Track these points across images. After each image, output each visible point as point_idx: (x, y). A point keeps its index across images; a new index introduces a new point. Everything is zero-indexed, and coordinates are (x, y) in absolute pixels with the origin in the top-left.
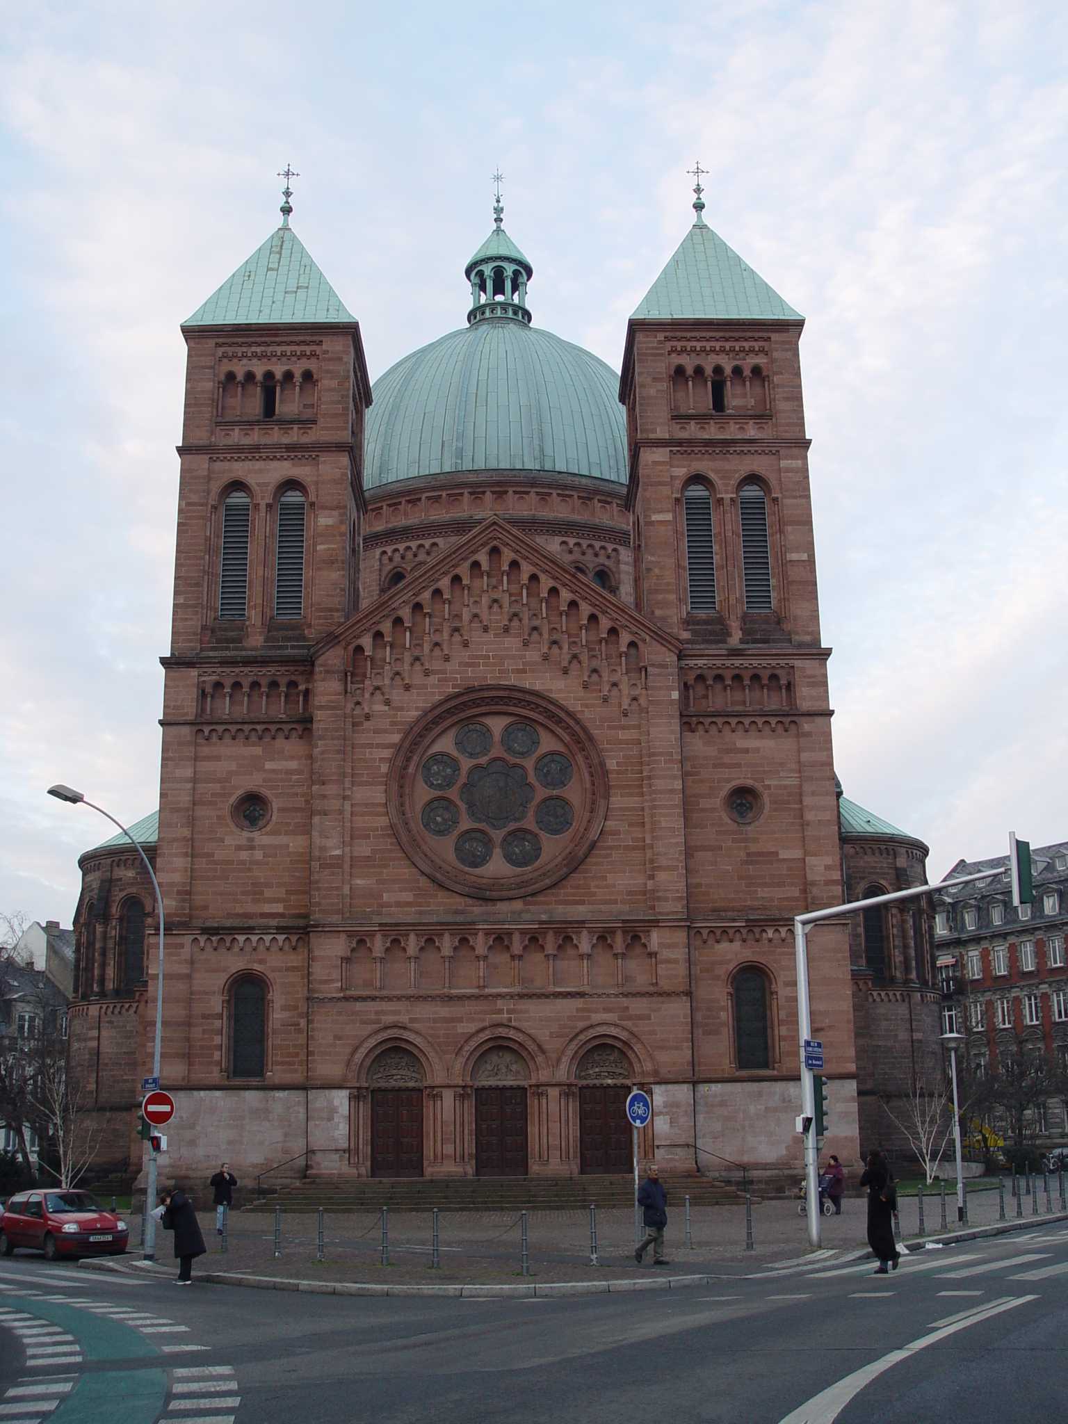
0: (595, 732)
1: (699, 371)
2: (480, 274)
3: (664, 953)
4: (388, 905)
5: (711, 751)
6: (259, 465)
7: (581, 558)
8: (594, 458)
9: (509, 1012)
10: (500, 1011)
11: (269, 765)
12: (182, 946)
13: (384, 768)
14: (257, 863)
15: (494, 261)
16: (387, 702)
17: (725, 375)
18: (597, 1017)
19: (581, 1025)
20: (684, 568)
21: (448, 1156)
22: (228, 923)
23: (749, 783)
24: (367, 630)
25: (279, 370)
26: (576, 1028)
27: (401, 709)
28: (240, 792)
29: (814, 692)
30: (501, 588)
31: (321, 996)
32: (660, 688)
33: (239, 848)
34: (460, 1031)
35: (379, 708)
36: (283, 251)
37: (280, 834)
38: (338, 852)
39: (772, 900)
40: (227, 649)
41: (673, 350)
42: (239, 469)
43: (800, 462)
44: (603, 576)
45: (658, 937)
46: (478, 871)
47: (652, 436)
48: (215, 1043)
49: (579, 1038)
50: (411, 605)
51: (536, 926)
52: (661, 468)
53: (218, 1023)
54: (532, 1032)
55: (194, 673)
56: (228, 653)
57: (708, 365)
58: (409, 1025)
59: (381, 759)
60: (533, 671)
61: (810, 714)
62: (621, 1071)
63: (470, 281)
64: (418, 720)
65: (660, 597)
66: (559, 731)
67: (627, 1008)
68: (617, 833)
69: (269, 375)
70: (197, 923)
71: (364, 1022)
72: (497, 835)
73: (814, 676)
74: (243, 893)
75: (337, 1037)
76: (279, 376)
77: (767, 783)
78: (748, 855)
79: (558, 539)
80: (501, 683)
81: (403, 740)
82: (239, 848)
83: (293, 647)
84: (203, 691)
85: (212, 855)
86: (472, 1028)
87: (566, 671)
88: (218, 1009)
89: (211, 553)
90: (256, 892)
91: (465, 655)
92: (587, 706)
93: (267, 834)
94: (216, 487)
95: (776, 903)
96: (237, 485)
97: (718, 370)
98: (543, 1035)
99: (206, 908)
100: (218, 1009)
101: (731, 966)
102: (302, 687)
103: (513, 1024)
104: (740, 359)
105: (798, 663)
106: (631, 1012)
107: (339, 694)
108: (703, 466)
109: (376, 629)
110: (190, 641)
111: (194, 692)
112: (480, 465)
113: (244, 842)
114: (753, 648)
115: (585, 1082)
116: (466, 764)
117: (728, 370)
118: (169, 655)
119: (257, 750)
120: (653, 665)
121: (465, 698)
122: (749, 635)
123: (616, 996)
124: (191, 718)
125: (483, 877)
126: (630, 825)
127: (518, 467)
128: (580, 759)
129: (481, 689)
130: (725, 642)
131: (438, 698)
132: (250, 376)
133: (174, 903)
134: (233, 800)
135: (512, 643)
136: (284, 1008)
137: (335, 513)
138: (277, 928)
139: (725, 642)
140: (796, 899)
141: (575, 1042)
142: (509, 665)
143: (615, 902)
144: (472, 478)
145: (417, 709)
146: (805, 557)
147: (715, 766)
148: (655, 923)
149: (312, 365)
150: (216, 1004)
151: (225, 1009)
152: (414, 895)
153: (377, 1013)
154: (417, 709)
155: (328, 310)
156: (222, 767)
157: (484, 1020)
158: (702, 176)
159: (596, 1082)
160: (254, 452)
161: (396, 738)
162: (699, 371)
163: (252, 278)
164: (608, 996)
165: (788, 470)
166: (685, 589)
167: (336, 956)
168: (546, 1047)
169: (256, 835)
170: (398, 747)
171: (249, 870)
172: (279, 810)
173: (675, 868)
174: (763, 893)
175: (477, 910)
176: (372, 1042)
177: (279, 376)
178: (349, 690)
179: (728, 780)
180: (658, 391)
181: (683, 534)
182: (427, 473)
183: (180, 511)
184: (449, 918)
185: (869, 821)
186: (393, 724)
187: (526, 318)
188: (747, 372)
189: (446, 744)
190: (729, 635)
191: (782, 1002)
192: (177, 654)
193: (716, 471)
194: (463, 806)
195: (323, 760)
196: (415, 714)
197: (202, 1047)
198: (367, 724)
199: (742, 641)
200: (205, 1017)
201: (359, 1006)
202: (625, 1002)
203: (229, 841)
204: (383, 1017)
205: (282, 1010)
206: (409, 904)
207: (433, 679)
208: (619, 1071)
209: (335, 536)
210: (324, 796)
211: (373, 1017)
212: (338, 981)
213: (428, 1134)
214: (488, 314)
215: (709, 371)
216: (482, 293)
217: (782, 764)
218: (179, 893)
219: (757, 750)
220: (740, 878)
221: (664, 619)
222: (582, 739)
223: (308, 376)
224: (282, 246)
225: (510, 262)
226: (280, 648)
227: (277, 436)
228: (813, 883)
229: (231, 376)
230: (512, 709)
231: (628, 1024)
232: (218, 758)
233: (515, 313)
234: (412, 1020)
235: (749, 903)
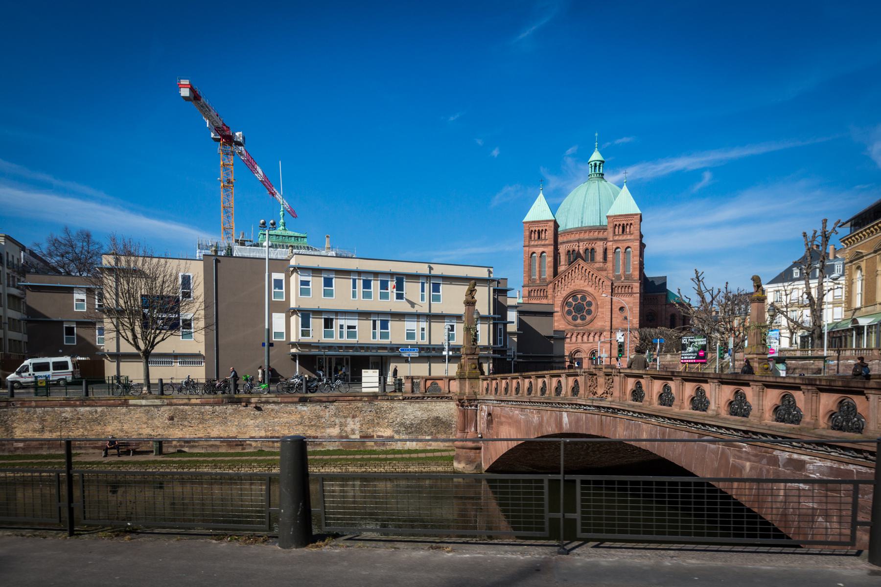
35: (559, 294)
42: (534, 249)
69: (539, 230)
72: (579, 316)
97: (623, 224)
98: (585, 349)
111: (527, 292)
112: (587, 225)
114: (625, 281)
116: (574, 303)
132: (535, 231)
135: (582, 282)
142: (581, 286)
144: (584, 228)
148: (605, 331)
149: (547, 228)
160: (537, 246)
161: (562, 299)
175: (575, 328)
189: (571, 300)
222: (595, 298)
223: (546, 230)
227: (540, 242)
229: (532, 231)
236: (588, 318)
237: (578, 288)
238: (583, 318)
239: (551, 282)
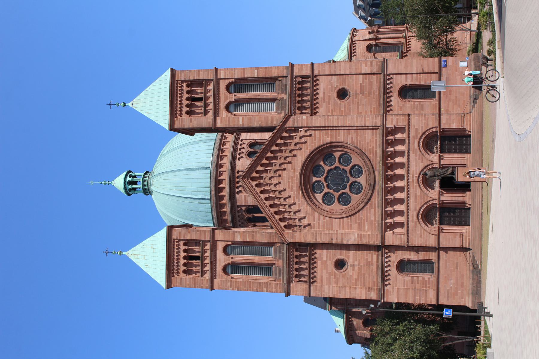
0: (316, 146)
1: (187, 106)
2: (130, 190)
3: (394, 123)
4: (375, 218)
5: (324, 105)
6: (218, 262)
7: (245, 154)
8: (206, 148)
9: (413, 176)
10: (413, 180)
11: (325, 259)
12: (387, 290)
13: (327, 219)
14: (359, 263)
15: (126, 185)
16: (304, 218)
17: (189, 97)
18: (416, 147)
19: (419, 152)
20: (259, 113)
21: (463, 199)
22: (380, 274)
23: (336, 92)
24: (279, 224)
25: (183, 254)
27: (306, 212)
28: (334, 269)
29: (304, 69)
30: (265, 177)
31: (406, 242)
32: (302, 123)
33: (353, 270)
34: (420, 194)
36: (137, 254)
37: (349, 255)
38: (356, 235)
39: (377, 85)
40: (283, 273)
41: (181, 114)
43: (222, 71)
44: (251, 145)
45: (389, 125)
46: (364, 187)
47: (211, 123)
48: (422, 279)
49: (423, 153)
50: (270, 208)
51: (384, 167)
52: (223, 121)
53: (415, 278)
54: (420, 170)
55: (291, 284)
56: (285, 273)
57: (185, 102)
58: (417, 211)
59: (324, 219)
60: (294, 167)
61: (313, 70)
62: (435, 139)
63: (132, 194)
64: (310, 206)
65: (269, 122)
66: (315, 158)
67: (413, 136)
68: (352, 138)
69: (185, 258)
70: (380, 284)
71: (416, 227)
73: (299, 69)
74: (369, 267)
75: (421, 236)
76: (185, 254)
77: (336, 86)
78: (361, 93)
79: (237, 161)
80: (298, 177)
81: (317, 212)
82: (353, 270)
83: (283, 250)
84: (298, 282)
85: (356, 279)
86: (418, 189)
87: (295, 156)
88: (410, 278)
89: (248, 278)
90: (370, 264)
91: (287, 189)
92: (307, 148)
93: (349, 259)
94: (225, 277)
95: (378, 84)
96: (225, 269)
97: (187, 99)
98: (422, 166)
99: (374, 282)
100: (410, 278)
101: (400, 100)
102: (298, 247)
103: (418, 175)
104: (184, 92)
105: (295, 74)
106: (415, 135)
107: (301, 234)
108: (222, 105)
109: (278, 220)
110: (280, 286)
111: (299, 284)
113: (352, 268)
115: (439, 152)
116: (326, 190)
117: (188, 96)
118: (285, 294)
119: (319, 263)
120: (294, 124)
121: (304, 190)
122: (284, 91)
123: (409, 140)
124: (307, 286)
125: (366, 185)
126: (349, 134)
127: (209, 175)
128: (325, 151)
129: (301, 184)
130: (286, 100)
131: (303, 199)
132: (185, 265)
133: (372, 293)
134: (336, 272)
136: (410, 255)
137: (236, 234)
138: (382, 256)
139: (286, 100)
140: (377, 78)
141: (424, 154)
142: (292, 174)
143: (376, 140)
144: (213, 193)
145: (306, 207)
146: (256, 71)
147: (329, 104)
148: (384, 125)
150: (408, 279)
151: (410, 275)
152: (372, 209)
153: (413, 222)
154: (306, 207)
155: (161, 237)
156: (325, 275)
157: (416, 186)
158: (112, 103)
159: (438, 148)
161: (317, 214)
162: (187, 106)
163: (147, 265)
164: (409, 143)
165: (225, 76)
166: (266, 113)
167: (392, 236)
168: (426, 165)
169: (349, 264)
170: (320, 214)
171: (361, 266)
172: (340, 255)
173: (365, 119)
174: (374, 89)
176: (423, 224)
177: (185, 254)
178: (299, 230)
179: (334, 100)
180: (195, 121)
181: (247, 113)
182: (210, 209)
183: (233, 289)
184: (380, 196)
185: (343, 50)
186: (312, 215)
187: (147, 173)
188: (189, 89)
190: (283, 98)
191: (412, 83)
192: (284, 291)
193: (225, 101)
194: (342, 191)
195: (323, 239)
196: (308, 207)
197: (423, 284)
198: (312, 224)
199: (286, 94)
200: (412, 283)
201: (410, 229)
202: (411, 136)
203: (351, 273)
204: (414, 220)
205: (411, 256)
206: (375, 211)
207: (296, 201)
208: (435, 140)
209: (244, 235)
210: (337, 239)
211: (414, 224)
212: (401, 236)
213: (455, 206)
214: (146, 187)
215: (188, 102)
216: (136, 190)
217: (330, 81)
218: (369, 291)
219: (324, 90)
220: (369, 97)
221: (277, 121)
223: (185, 244)
224: (135, 254)
225: (126, 179)
226: (283, 254)
228: (372, 70)
229: (184, 272)
230: (308, 174)
231: (419, 136)
232: (322, 277)
233: (146, 177)
234: (415, 210)
235: (378, 93)
236: (356, 160)
237: (296, 181)
238: (356, 171)
239: (282, 235)
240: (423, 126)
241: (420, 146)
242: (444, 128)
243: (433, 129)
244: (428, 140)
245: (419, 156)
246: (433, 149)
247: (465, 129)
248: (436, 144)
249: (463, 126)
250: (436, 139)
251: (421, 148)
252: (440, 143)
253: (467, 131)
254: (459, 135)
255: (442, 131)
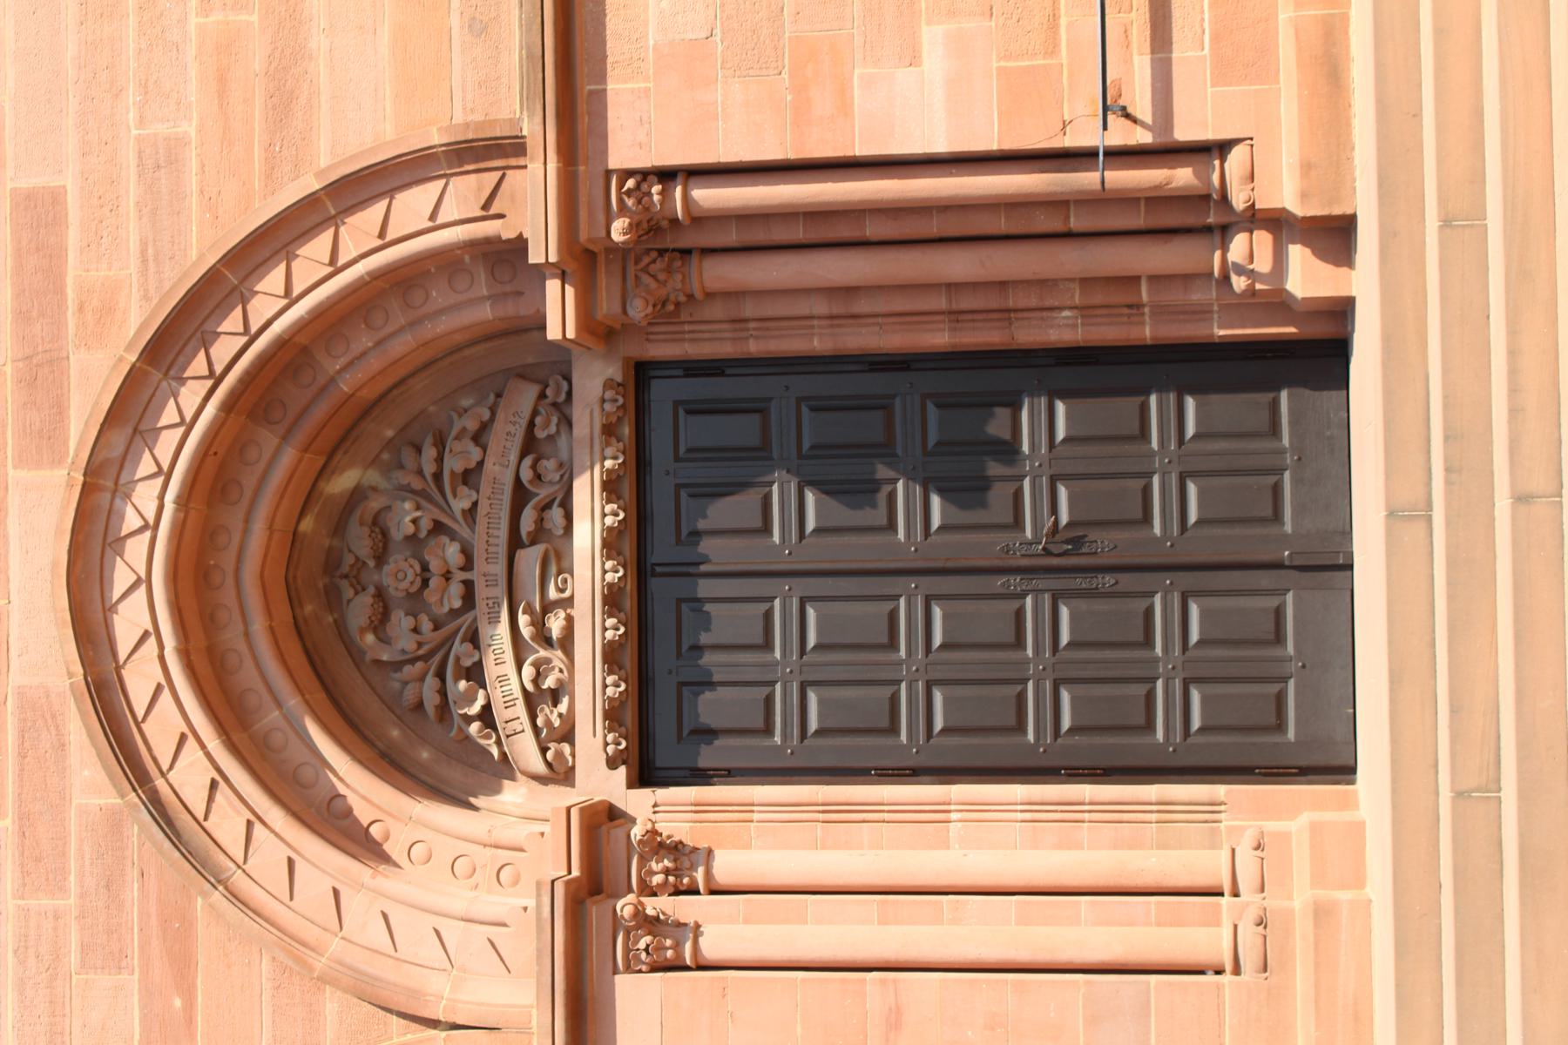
26: (114, 822)
49: (196, 798)
159: (586, 649)
208: (502, 464)
240: (190, 129)
241: (129, 621)
242: (667, 175)
243: (413, 205)
244: (343, 482)
245: (111, 884)
246: (475, 674)
247: (1182, 176)
248: (529, 559)
249: (1143, 107)
250: (530, 445)
251: (140, 680)
252: (611, 544)
253: (1256, 218)
254: (1064, 330)
255: (619, 230)
